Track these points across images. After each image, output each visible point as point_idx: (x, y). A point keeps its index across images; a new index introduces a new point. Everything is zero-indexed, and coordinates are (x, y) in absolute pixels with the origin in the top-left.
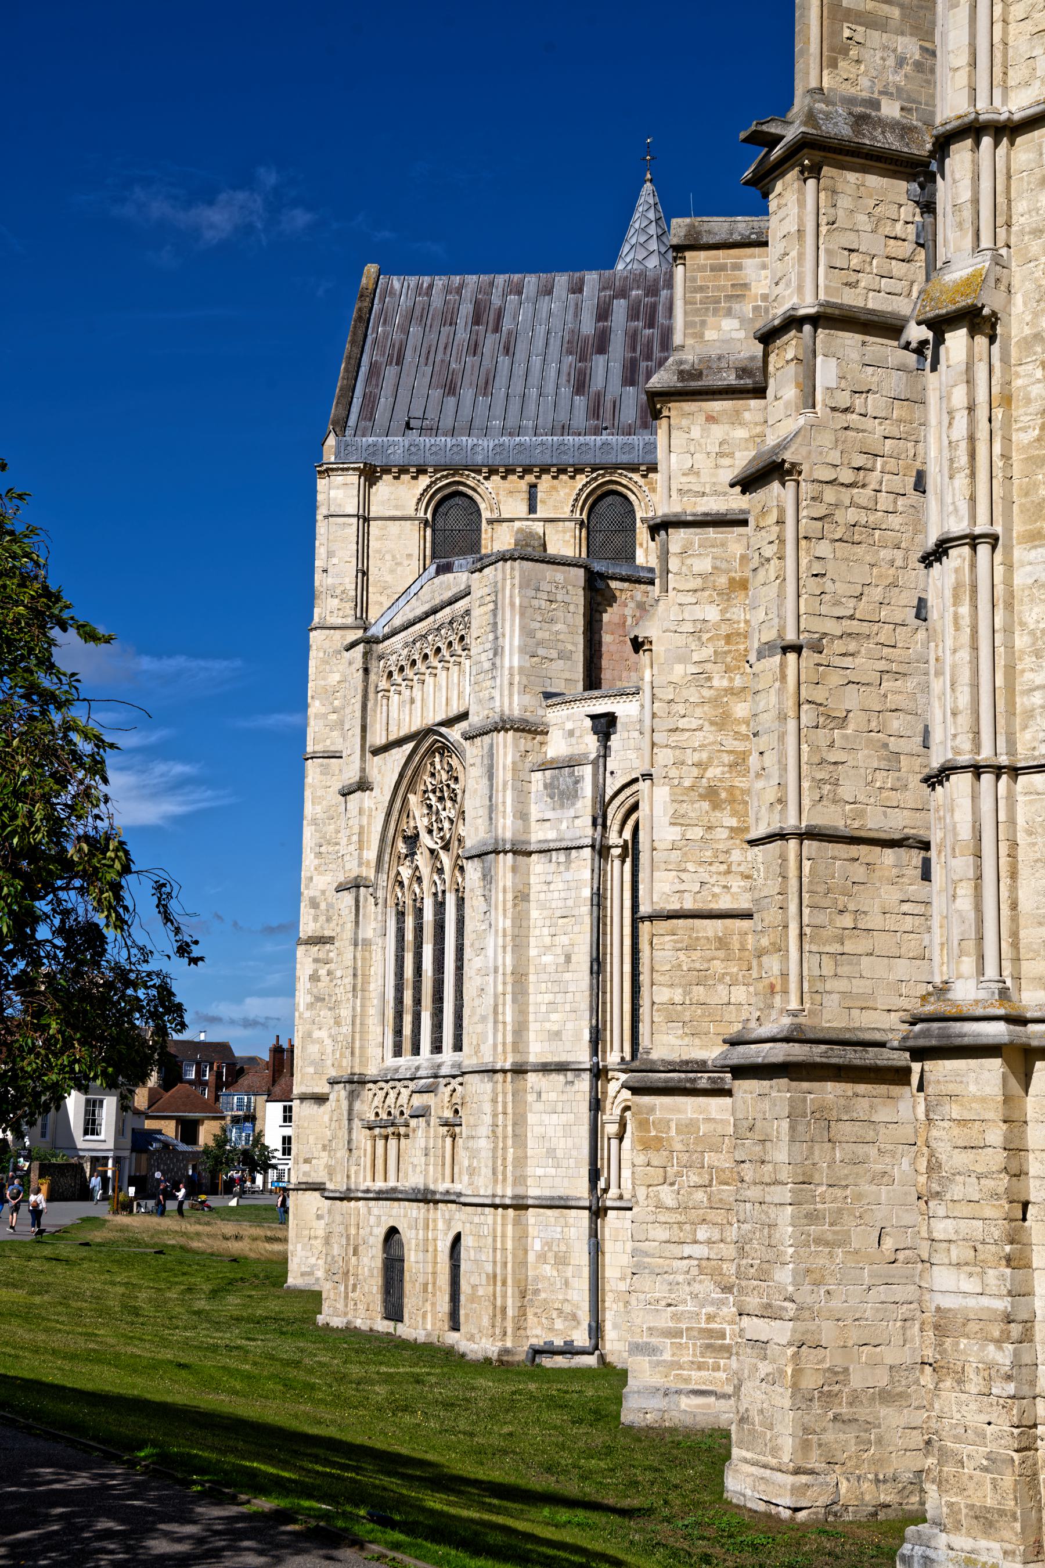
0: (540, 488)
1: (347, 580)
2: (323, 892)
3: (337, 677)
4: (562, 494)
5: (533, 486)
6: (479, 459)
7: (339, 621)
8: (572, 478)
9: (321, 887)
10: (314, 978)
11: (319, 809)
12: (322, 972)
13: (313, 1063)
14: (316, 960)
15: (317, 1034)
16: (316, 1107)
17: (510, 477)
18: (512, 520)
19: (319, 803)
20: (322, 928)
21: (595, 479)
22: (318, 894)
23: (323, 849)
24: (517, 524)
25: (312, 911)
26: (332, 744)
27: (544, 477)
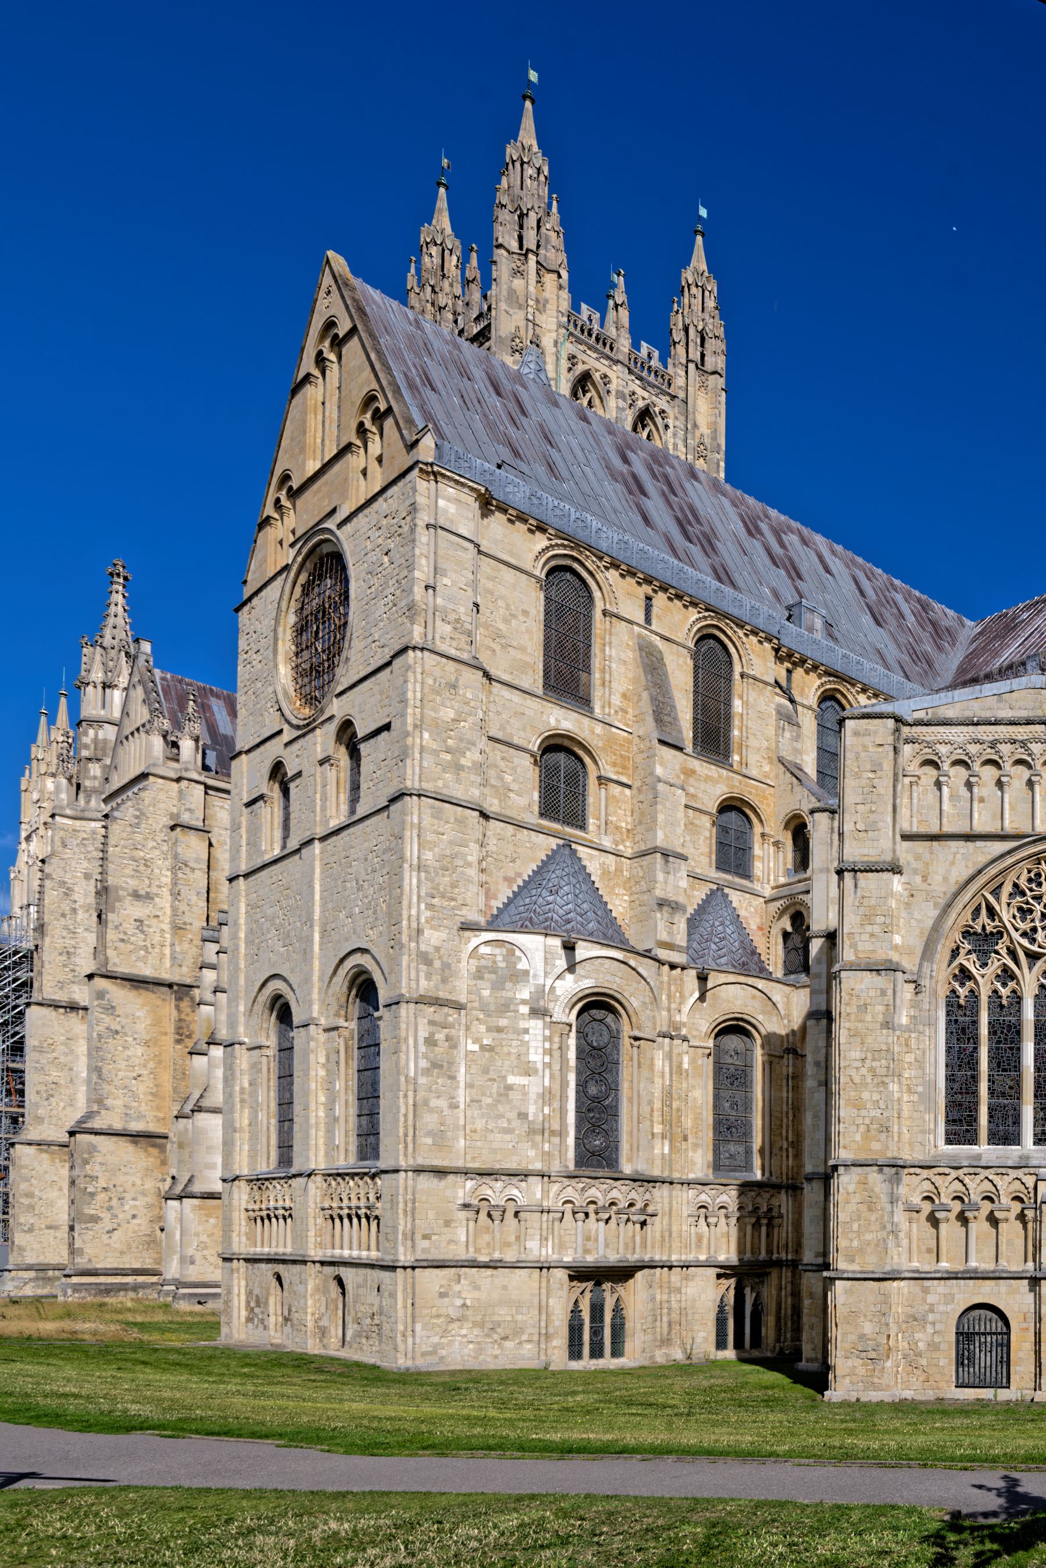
1: (462, 610)
2: (437, 949)
3: (451, 714)
7: (453, 652)
9: (434, 942)
10: (430, 1042)
12: (440, 1036)
13: (429, 1134)
14: (432, 1023)
15: (434, 1103)
19: (430, 849)
20: (436, 987)
23: (435, 901)
26: (445, 786)
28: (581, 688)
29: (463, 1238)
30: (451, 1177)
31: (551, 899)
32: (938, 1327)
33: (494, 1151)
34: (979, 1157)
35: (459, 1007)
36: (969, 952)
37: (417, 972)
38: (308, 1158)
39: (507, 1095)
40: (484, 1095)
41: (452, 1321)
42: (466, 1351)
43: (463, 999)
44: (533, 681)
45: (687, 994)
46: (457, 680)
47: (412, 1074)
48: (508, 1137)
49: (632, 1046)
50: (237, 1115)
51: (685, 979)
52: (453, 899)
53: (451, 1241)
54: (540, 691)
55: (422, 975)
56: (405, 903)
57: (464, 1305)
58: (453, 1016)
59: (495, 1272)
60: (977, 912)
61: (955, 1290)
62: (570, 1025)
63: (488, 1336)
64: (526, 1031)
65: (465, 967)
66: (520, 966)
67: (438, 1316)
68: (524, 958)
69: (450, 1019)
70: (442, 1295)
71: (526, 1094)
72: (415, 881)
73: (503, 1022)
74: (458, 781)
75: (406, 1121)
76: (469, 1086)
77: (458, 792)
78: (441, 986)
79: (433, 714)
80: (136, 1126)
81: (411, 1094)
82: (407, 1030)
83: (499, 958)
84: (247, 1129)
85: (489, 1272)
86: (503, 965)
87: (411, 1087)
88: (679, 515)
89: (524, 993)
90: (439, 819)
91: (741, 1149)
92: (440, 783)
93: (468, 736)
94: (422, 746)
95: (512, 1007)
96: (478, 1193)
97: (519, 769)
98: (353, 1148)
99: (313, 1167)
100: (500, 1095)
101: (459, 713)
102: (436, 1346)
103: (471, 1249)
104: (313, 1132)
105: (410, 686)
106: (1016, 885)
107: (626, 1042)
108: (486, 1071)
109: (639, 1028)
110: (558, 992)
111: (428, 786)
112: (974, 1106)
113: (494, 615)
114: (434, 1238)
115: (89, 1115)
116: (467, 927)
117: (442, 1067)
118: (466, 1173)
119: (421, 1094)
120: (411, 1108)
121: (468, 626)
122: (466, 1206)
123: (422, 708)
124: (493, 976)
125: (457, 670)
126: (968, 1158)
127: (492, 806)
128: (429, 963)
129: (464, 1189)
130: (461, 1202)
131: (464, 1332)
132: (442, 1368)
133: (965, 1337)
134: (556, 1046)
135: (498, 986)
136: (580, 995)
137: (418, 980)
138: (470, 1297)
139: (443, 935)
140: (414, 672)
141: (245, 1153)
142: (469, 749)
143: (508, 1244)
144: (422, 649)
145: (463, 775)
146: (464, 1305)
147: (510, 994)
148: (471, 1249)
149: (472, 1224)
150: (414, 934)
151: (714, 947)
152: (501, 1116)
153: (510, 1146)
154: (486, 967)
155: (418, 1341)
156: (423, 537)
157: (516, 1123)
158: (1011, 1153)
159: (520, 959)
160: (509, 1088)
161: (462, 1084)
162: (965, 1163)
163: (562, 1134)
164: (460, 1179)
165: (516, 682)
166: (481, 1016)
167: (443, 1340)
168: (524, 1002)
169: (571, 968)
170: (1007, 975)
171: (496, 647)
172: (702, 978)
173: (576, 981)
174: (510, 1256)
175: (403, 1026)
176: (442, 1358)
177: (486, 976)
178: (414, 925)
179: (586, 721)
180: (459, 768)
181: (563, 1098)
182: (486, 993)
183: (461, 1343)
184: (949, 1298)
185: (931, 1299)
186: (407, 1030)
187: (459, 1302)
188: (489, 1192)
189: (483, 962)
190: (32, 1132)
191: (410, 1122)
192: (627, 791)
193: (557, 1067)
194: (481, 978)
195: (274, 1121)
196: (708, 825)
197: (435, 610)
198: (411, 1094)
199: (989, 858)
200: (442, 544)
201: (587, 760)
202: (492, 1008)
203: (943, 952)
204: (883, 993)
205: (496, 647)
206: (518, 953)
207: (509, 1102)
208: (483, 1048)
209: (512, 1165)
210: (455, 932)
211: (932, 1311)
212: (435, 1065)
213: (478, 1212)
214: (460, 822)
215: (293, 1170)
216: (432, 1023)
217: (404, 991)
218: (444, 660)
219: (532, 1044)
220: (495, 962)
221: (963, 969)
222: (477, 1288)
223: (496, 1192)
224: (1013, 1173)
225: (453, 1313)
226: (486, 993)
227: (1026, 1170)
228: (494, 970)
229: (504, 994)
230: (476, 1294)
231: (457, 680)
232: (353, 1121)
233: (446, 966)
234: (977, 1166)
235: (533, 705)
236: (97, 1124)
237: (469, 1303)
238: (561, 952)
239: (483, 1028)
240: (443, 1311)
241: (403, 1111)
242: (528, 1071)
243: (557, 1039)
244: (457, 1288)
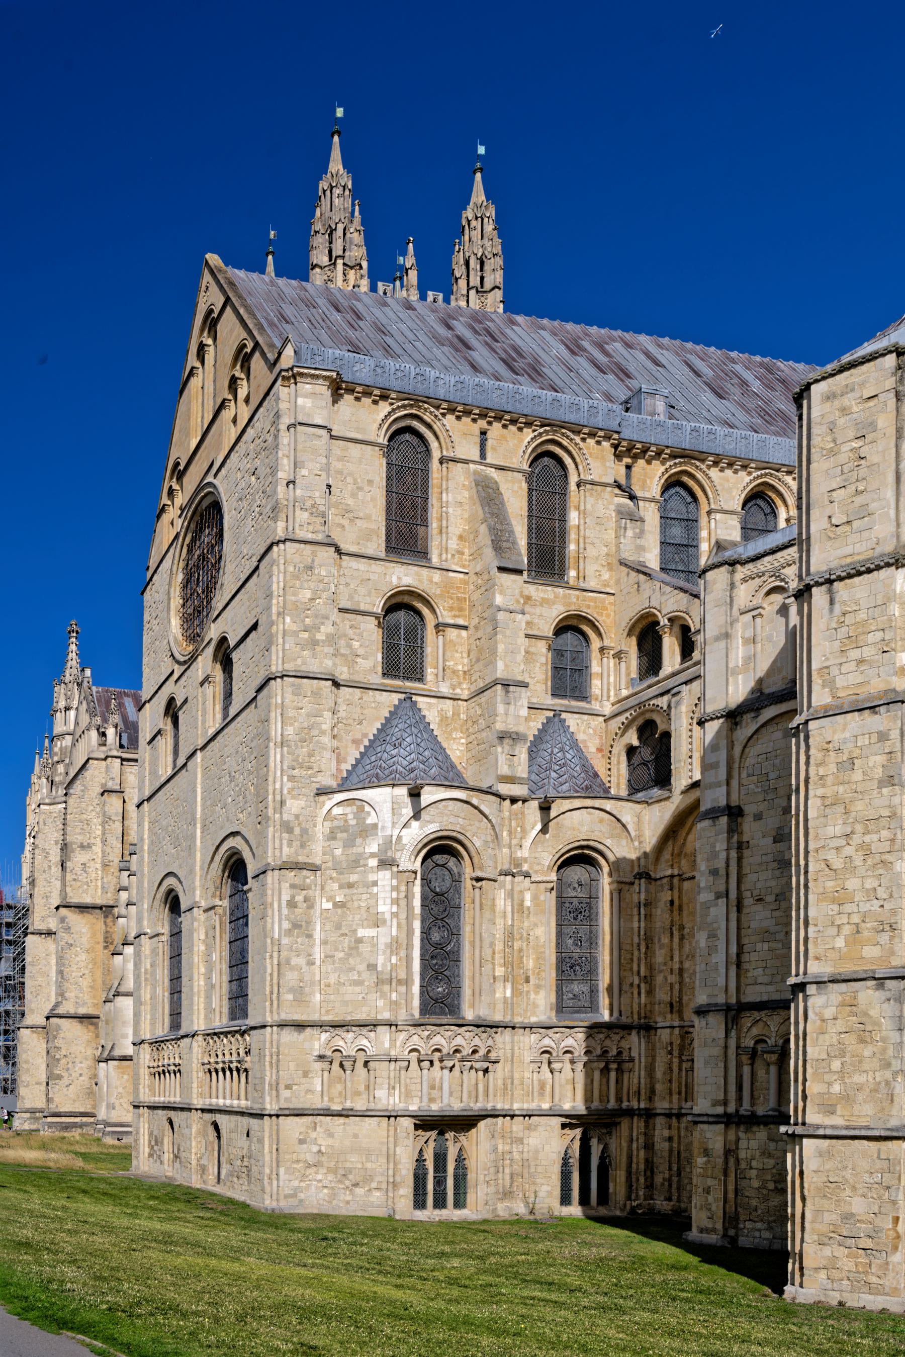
0: (489, 434)
2: (297, 816)
3: (308, 594)
4: (511, 444)
5: (483, 433)
7: (310, 536)
8: (520, 429)
9: (295, 810)
11: (290, 730)
12: (299, 898)
16: (296, 1034)
17: (464, 419)
18: (466, 462)
21: (540, 435)
22: (292, 818)
23: (295, 772)
24: (472, 466)
25: (285, 835)
26: (304, 663)
27: (495, 424)
28: (419, 542)
29: (319, 1088)
30: (308, 1030)
31: (394, 752)
33: (346, 1003)
35: (315, 869)
37: (281, 840)
38: (192, 1021)
39: (357, 948)
40: (336, 950)
41: (309, 1166)
42: (321, 1195)
43: (318, 861)
44: (377, 545)
45: (528, 828)
46: (313, 561)
47: (276, 936)
48: (358, 989)
49: (474, 887)
50: (142, 991)
51: (526, 812)
52: (310, 768)
53: (309, 1091)
54: (383, 555)
55: (285, 842)
56: (271, 779)
57: (320, 1151)
58: (309, 877)
59: (346, 1120)
62: (415, 872)
63: (340, 1182)
64: (375, 884)
65: (320, 829)
66: (369, 821)
67: (298, 1161)
68: (373, 813)
69: (308, 881)
70: (301, 1142)
71: (375, 945)
72: (279, 756)
73: (353, 878)
74: (314, 656)
75: (272, 980)
76: (324, 942)
77: (314, 667)
78: (300, 850)
79: (293, 598)
80: (82, 1011)
81: (275, 954)
82: (273, 895)
83: (350, 816)
84: (149, 1002)
85: (342, 1120)
86: (353, 822)
87: (276, 948)
88: (504, 356)
89: (373, 847)
90: (298, 695)
92: (299, 661)
93: (323, 612)
94: (284, 631)
95: (362, 862)
96: (331, 1044)
97: (365, 634)
98: (226, 1010)
99: (196, 1028)
100: (350, 948)
101: (314, 592)
102: (297, 1190)
103: (326, 1099)
104: (196, 998)
105: (275, 579)
107: (468, 884)
108: (338, 927)
109: (481, 869)
110: (405, 841)
111: (290, 667)
113: (344, 494)
114: (295, 1087)
115: (57, 1005)
116: (322, 792)
117: (301, 927)
118: (321, 1026)
119: (284, 954)
120: (275, 967)
121: (322, 508)
122: (321, 1057)
123: (284, 595)
124: (345, 835)
125: (313, 552)
127: (343, 674)
128: (290, 830)
129: (319, 1041)
130: (316, 1053)
131: (319, 1177)
132: (301, 1211)
134: (402, 895)
135: (349, 844)
136: (425, 841)
137: (281, 849)
138: (325, 1143)
139: (302, 803)
140: (278, 566)
141: (148, 1022)
142: (323, 624)
143: (358, 1094)
144: (284, 542)
145: (318, 649)
146: (320, 1151)
147: (360, 850)
148: (326, 1099)
149: (326, 1074)
150: (278, 806)
151: (554, 775)
152: (352, 969)
153: (360, 998)
154: (338, 827)
155: (281, 1184)
156: (285, 439)
157: (366, 975)
159: (369, 813)
160: (359, 941)
161: (318, 942)
163: (408, 982)
164: (315, 1031)
165: (363, 551)
166: (334, 875)
167: (302, 1184)
168: (373, 855)
169: (417, 816)
171: (345, 522)
172: (545, 808)
173: (421, 828)
174: (360, 1105)
175: (269, 892)
176: (301, 1201)
177: (339, 835)
178: (278, 798)
179: (425, 572)
180: (315, 643)
181: (409, 946)
182: (338, 852)
183: (317, 1187)
186: (273, 895)
187: (315, 1149)
188: (341, 1043)
189: (336, 823)
190: (29, 1020)
191: (275, 981)
192: (464, 633)
193: (403, 916)
195: (167, 994)
196: (544, 650)
197: (295, 501)
198: (275, 954)
200: (301, 438)
201: (425, 611)
202: (344, 865)
205: (345, 522)
206: (367, 808)
207: (359, 954)
208: (336, 905)
209: (361, 1015)
210: (312, 799)
212: (296, 926)
213: (331, 1063)
214: (316, 694)
216: (293, 886)
217: (270, 860)
218: (302, 546)
219: (381, 895)
220: (346, 821)
222: (331, 1135)
223: (348, 1042)
225: (310, 1159)
226: (338, 852)
228: (345, 829)
229: (355, 850)
230: (330, 1141)
231: (313, 561)
232: (226, 986)
233: (304, 831)
235: (377, 568)
236: (61, 1011)
237: (323, 1149)
238: (407, 800)
239: (335, 886)
240: (302, 1157)
241: (269, 971)
242: (377, 922)
243: (403, 888)
244: (314, 1135)
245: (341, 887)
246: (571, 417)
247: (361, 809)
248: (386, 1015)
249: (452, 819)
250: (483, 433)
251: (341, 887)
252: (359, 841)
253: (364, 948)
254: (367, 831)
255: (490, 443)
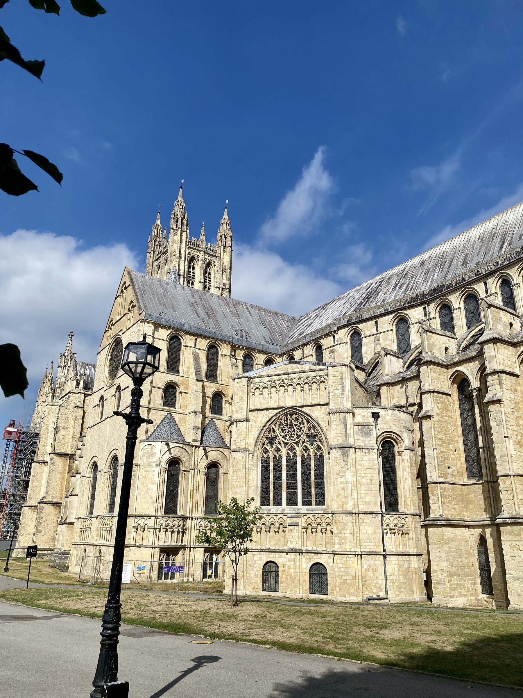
5: (196, 339)
6: (185, 328)
32: (258, 569)
34: (270, 510)
36: (268, 444)
48: (147, 505)
60: (269, 432)
61: (263, 556)
73: (148, 469)
86: (150, 451)
89: (155, 459)
91: (214, 506)
106: (281, 422)
108: (143, 484)
112: (269, 493)
126: (267, 510)
133: (265, 573)
135: (148, 458)
147: (151, 460)
152: (145, 498)
157: (149, 500)
158: (279, 508)
160: (148, 489)
162: (266, 512)
168: (154, 462)
170: (278, 450)
184: (261, 559)
185: (256, 559)
189: (145, 451)
194: (144, 456)
199: (273, 415)
203: (260, 444)
204: (243, 458)
211: (256, 563)
215: (93, 516)
221: (266, 449)
224: (280, 516)
226: (145, 460)
227: (284, 514)
234: (269, 513)
245: (145, 471)
246: (219, 337)
247: (152, 448)
248: (154, 514)
249: (178, 452)
250: (196, 339)
251: (145, 471)
252: (151, 457)
253: (150, 491)
254: (153, 455)
255: (197, 342)
